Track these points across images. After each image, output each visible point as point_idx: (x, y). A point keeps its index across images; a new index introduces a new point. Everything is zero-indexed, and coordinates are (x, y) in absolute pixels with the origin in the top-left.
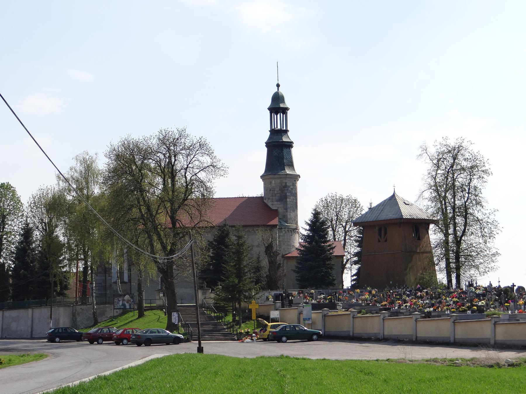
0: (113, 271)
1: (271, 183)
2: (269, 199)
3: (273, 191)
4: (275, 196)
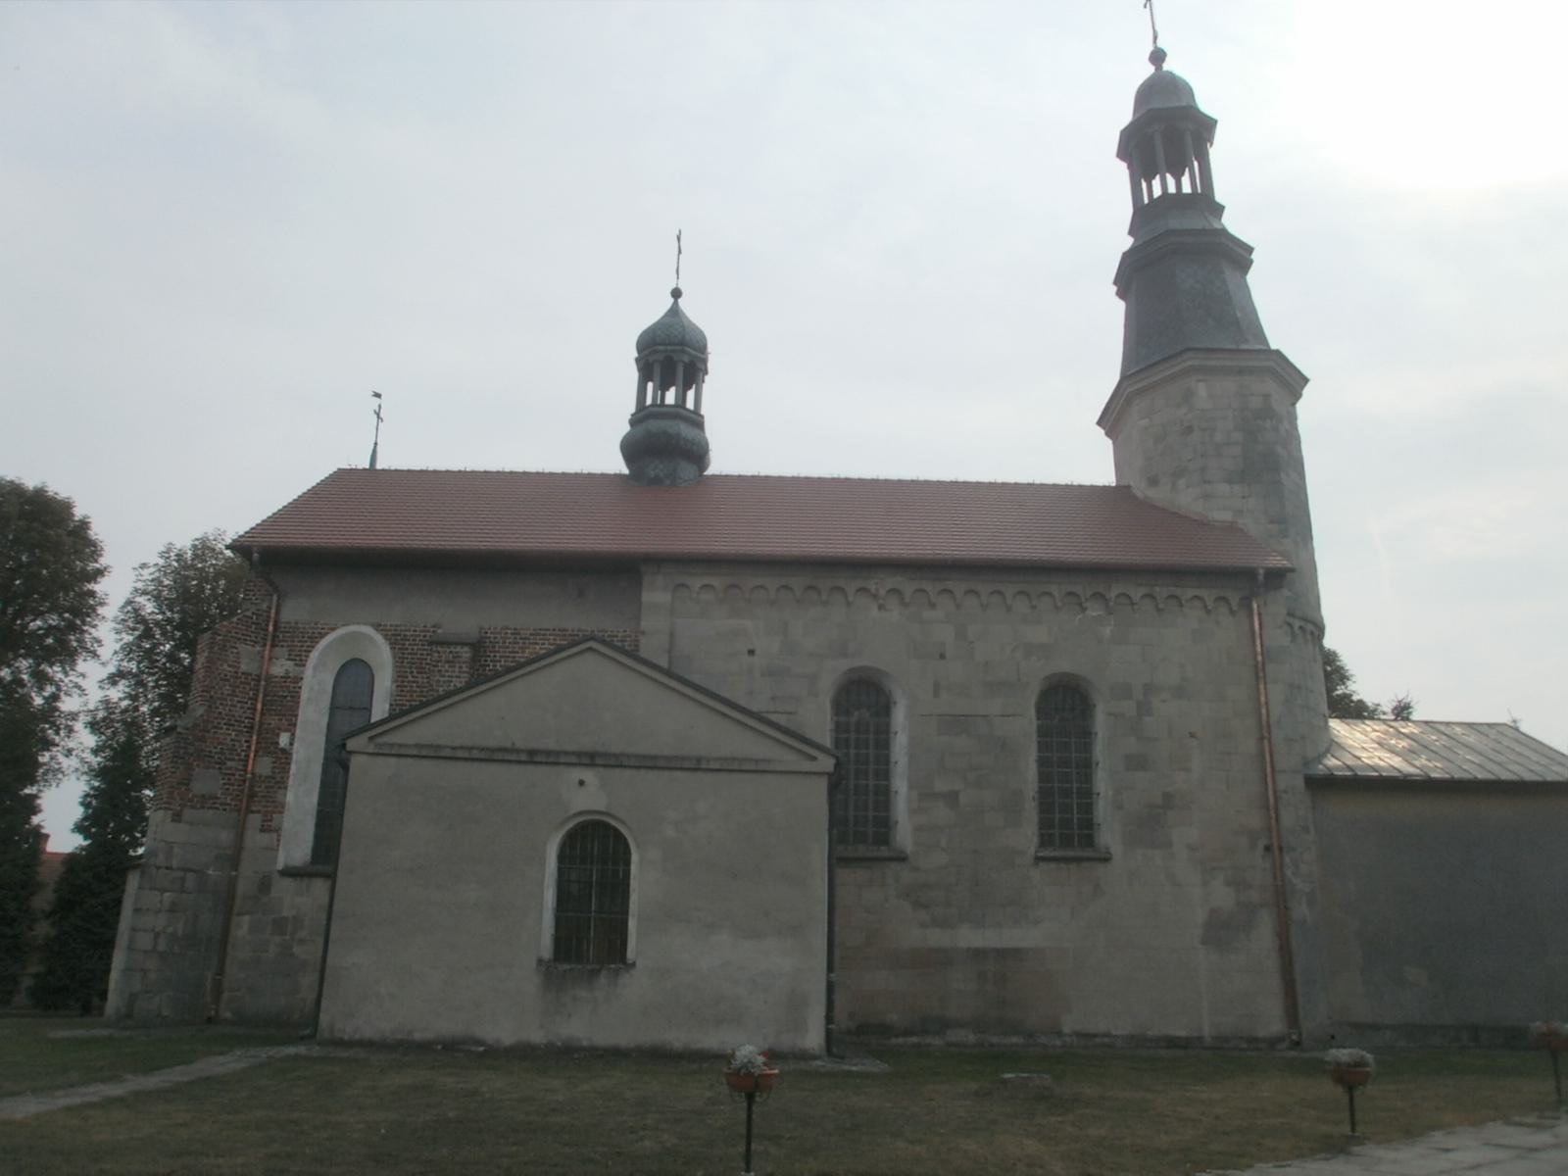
0: (290, 797)
1: (1188, 396)
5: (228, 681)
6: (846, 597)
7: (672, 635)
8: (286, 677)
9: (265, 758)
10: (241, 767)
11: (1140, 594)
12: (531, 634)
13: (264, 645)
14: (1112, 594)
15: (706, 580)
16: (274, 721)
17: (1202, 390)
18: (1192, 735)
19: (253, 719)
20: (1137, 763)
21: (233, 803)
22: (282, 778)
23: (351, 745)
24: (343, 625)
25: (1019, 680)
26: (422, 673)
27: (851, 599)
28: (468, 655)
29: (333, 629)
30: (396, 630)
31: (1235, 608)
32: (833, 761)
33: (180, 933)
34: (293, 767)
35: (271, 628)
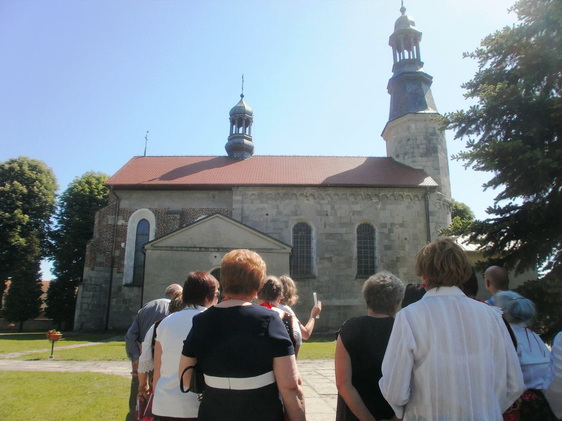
0: (125, 263)
1: (409, 128)
2: (406, 154)
3: (413, 140)
4: (418, 148)
5: (105, 227)
6: (297, 197)
7: (242, 210)
8: (122, 225)
9: (117, 251)
10: (110, 254)
11: (390, 194)
12: (198, 210)
13: (116, 215)
14: (381, 194)
15: (253, 192)
16: (119, 239)
17: (413, 126)
18: (406, 239)
19: (113, 239)
20: (388, 248)
21: (109, 264)
22: (123, 256)
23: (146, 247)
24: (139, 209)
25: (351, 222)
26: (164, 223)
27: (298, 197)
28: (179, 217)
29: (136, 210)
30: (156, 210)
31: (420, 199)
32: (291, 249)
33: (95, 303)
34: (126, 253)
35: (117, 210)
